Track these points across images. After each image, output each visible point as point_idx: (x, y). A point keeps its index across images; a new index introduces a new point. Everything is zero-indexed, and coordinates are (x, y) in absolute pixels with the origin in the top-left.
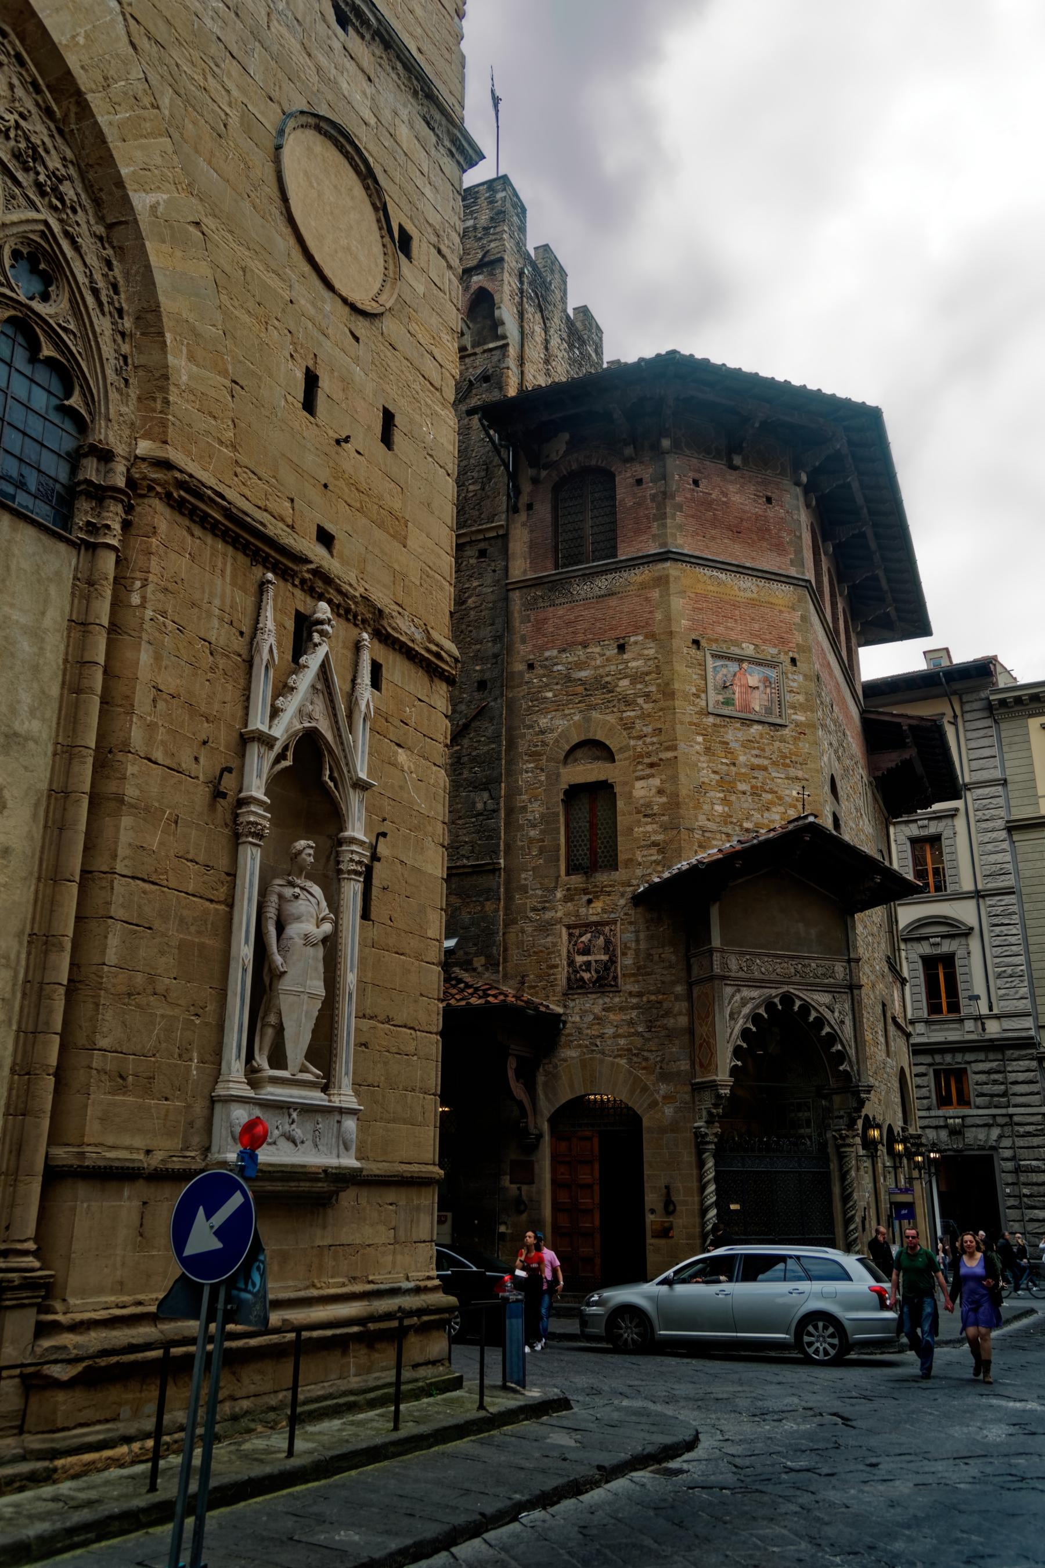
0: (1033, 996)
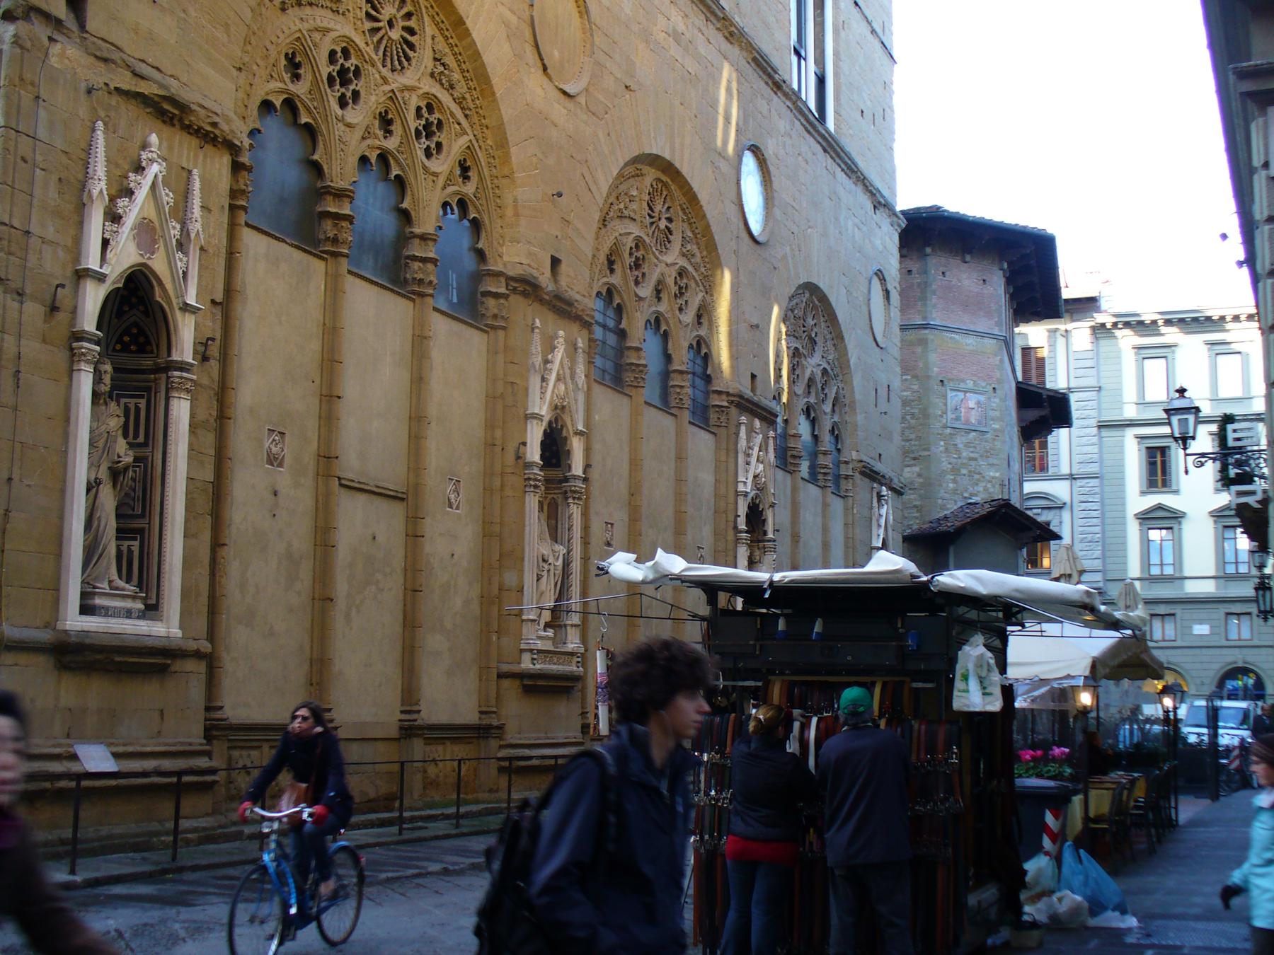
0: (1104, 557)
